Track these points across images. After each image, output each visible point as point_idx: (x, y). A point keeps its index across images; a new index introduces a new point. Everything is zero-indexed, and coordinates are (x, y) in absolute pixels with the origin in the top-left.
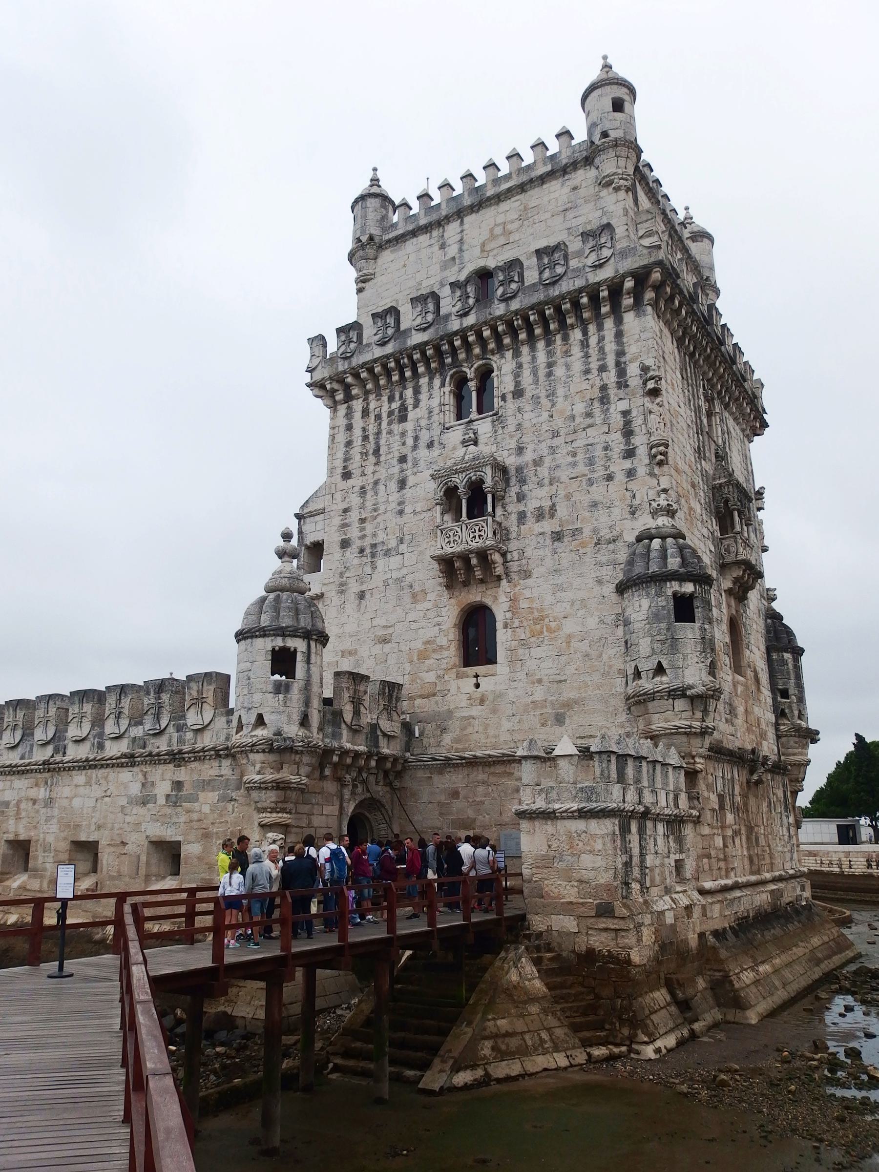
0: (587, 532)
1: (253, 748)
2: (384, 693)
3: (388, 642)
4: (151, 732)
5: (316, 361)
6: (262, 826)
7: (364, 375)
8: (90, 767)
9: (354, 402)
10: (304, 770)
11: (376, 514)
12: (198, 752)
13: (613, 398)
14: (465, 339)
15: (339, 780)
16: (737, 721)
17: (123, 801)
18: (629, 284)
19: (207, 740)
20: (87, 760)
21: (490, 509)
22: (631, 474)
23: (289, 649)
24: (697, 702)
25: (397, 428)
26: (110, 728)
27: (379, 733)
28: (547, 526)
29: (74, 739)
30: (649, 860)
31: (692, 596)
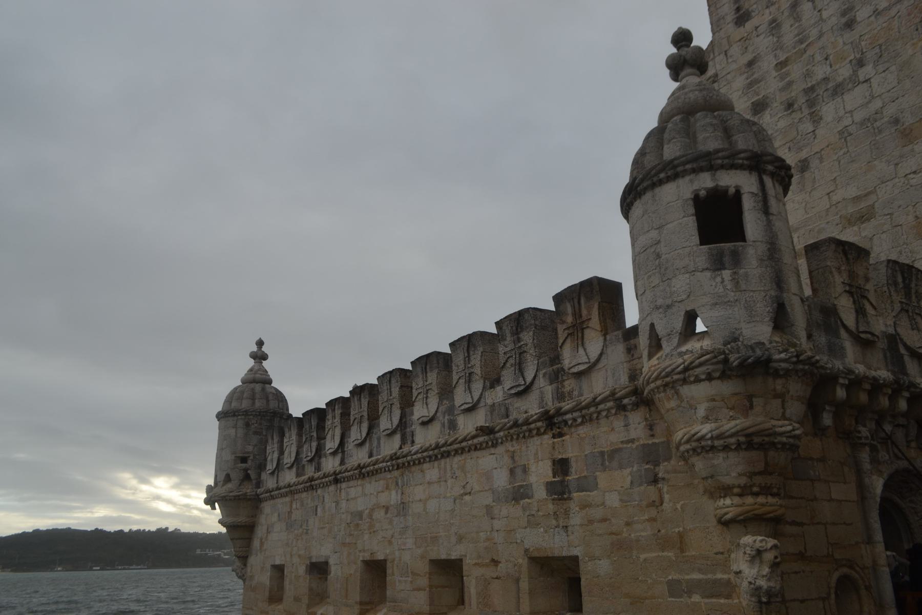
1: (686, 375)
2: (896, 284)
3: (868, 220)
4: (513, 391)
6: (725, 523)
8: (443, 456)
10: (796, 409)
11: (803, 46)
12: (587, 407)
17: (487, 499)
19: (599, 385)
20: (437, 446)
23: (725, 191)
26: (461, 397)
27: (903, 351)
29: (420, 421)
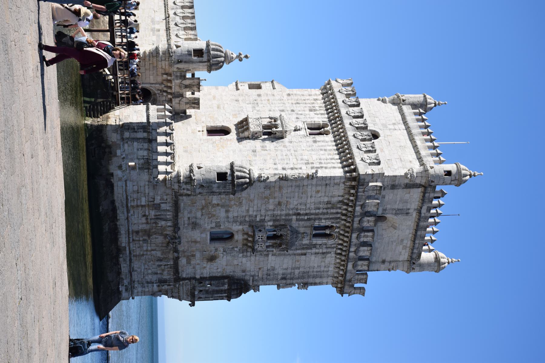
0: (254, 158)
1: (169, 45)
5: (341, 82)
7: (331, 96)
9: (322, 96)
13: (308, 166)
14: (340, 124)
15: (162, 83)
16: (190, 230)
18: (352, 167)
19: (173, 38)
21: (265, 130)
22: (276, 169)
24: (189, 179)
25: (308, 108)
26: (179, 11)
28: (258, 148)
30: (135, 144)
31: (227, 180)
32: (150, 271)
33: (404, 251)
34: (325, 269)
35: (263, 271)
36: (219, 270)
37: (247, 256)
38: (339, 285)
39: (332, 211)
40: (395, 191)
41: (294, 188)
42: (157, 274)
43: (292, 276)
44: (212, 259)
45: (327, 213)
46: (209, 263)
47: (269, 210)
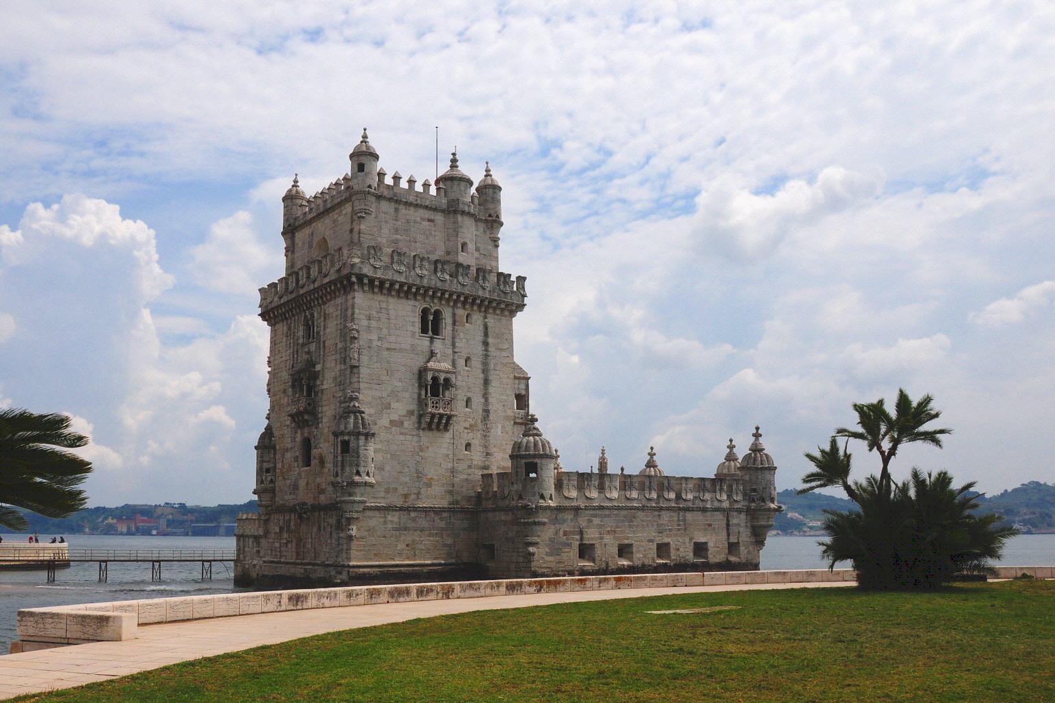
32: (329, 541)
33: (344, 212)
34: (339, 308)
35: (336, 392)
36: (332, 451)
37: (322, 418)
38: (345, 283)
39: (292, 328)
40: (296, 260)
41: (275, 380)
42: (331, 534)
43: (343, 351)
44: (322, 461)
45: (294, 333)
46: (326, 465)
47: (288, 400)
